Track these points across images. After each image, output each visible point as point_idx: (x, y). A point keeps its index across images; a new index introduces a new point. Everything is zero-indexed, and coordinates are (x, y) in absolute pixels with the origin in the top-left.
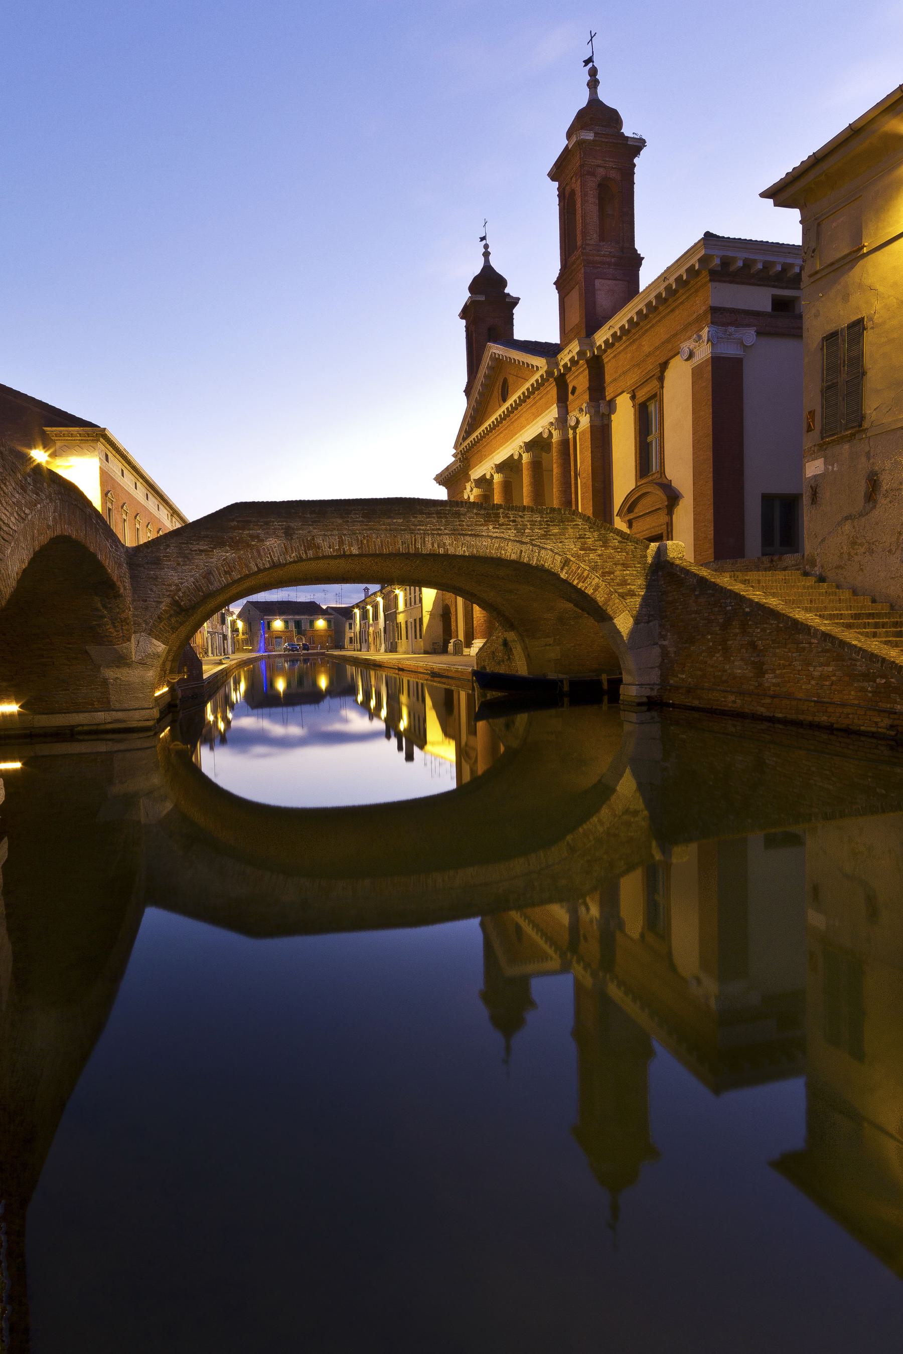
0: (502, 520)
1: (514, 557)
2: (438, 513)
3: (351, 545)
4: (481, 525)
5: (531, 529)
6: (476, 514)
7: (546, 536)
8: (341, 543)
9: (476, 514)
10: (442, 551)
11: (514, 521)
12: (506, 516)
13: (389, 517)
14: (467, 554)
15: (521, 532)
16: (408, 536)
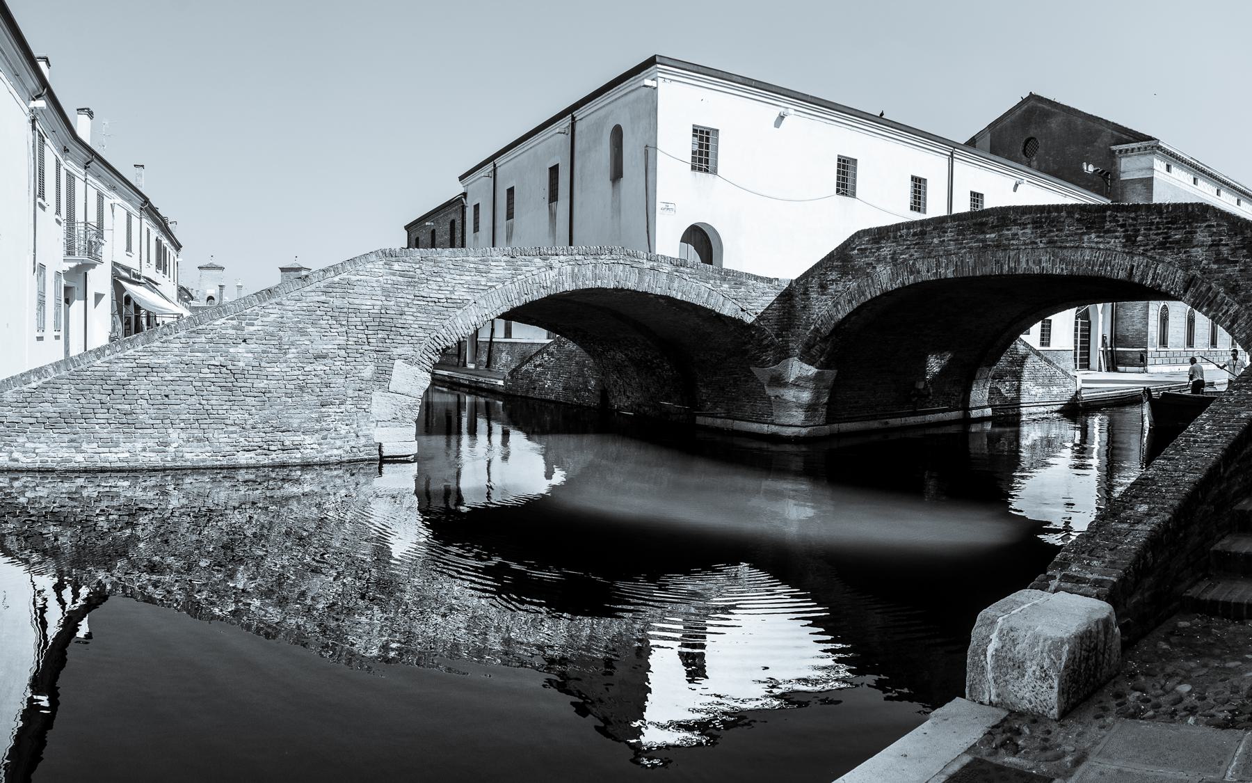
0: (1108, 225)
1: (1122, 275)
2: (1034, 222)
3: (947, 267)
4: (1083, 234)
5: (1145, 236)
6: (1078, 220)
7: (1162, 245)
8: (938, 266)
9: (1078, 220)
10: (1036, 270)
11: (1122, 226)
12: (1115, 220)
13: (984, 233)
14: (1065, 272)
15: (1130, 240)
16: (1000, 254)
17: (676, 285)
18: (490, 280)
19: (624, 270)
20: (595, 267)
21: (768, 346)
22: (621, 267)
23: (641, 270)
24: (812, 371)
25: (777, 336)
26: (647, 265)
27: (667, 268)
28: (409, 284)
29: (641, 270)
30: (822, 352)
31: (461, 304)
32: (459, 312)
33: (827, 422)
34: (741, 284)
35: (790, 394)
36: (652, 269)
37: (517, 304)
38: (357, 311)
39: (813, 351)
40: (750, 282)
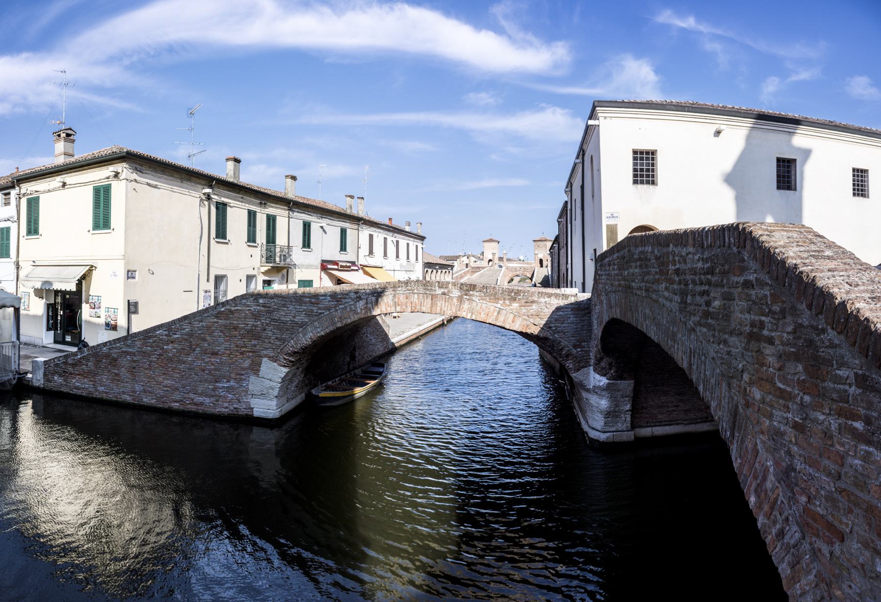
17: (466, 306)
18: (320, 309)
19: (418, 298)
20: (394, 296)
21: (568, 356)
22: (416, 296)
23: (433, 297)
24: (603, 381)
25: (575, 347)
26: (439, 291)
27: (456, 293)
28: (268, 312)
29: (433, 297)
30: (610, 364)
31: (303, 325)
32: (300, 330)
33: (633, 426)
34: (533, 302)
35: (593, 399)
36: (444, 294)
37: (339, 325)
38: (236, 328)
39: (603, 364)
40: (542, 300)
